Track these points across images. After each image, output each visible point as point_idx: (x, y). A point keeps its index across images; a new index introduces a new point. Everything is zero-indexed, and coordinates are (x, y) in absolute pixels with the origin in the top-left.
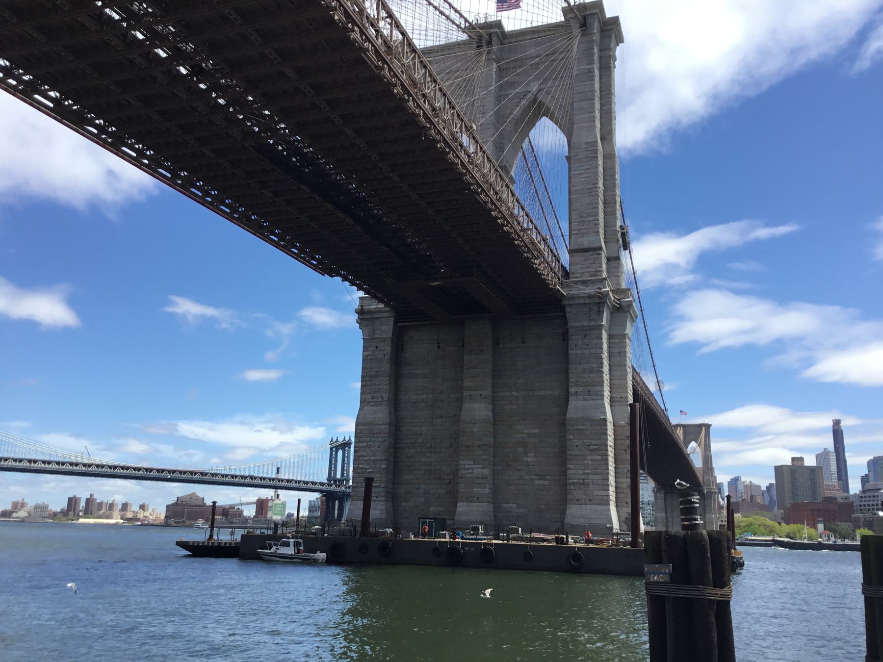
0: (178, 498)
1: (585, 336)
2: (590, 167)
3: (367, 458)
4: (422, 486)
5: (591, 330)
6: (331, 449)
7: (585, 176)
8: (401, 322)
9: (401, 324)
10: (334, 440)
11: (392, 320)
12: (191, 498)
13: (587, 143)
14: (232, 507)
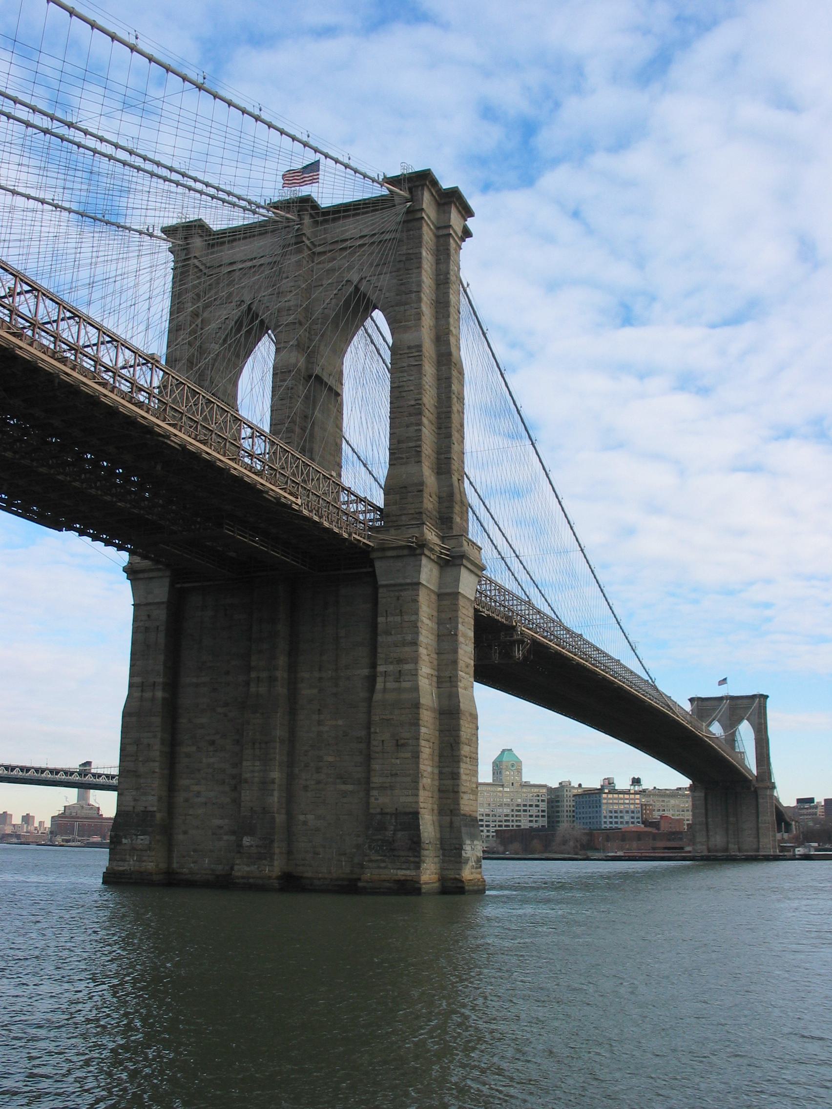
0: (65, 807)
1: (398, 599)
5: (405, 590)
8: (178, 583)
9: (178, 586)
11: (166, 582)
13: (409, 348)
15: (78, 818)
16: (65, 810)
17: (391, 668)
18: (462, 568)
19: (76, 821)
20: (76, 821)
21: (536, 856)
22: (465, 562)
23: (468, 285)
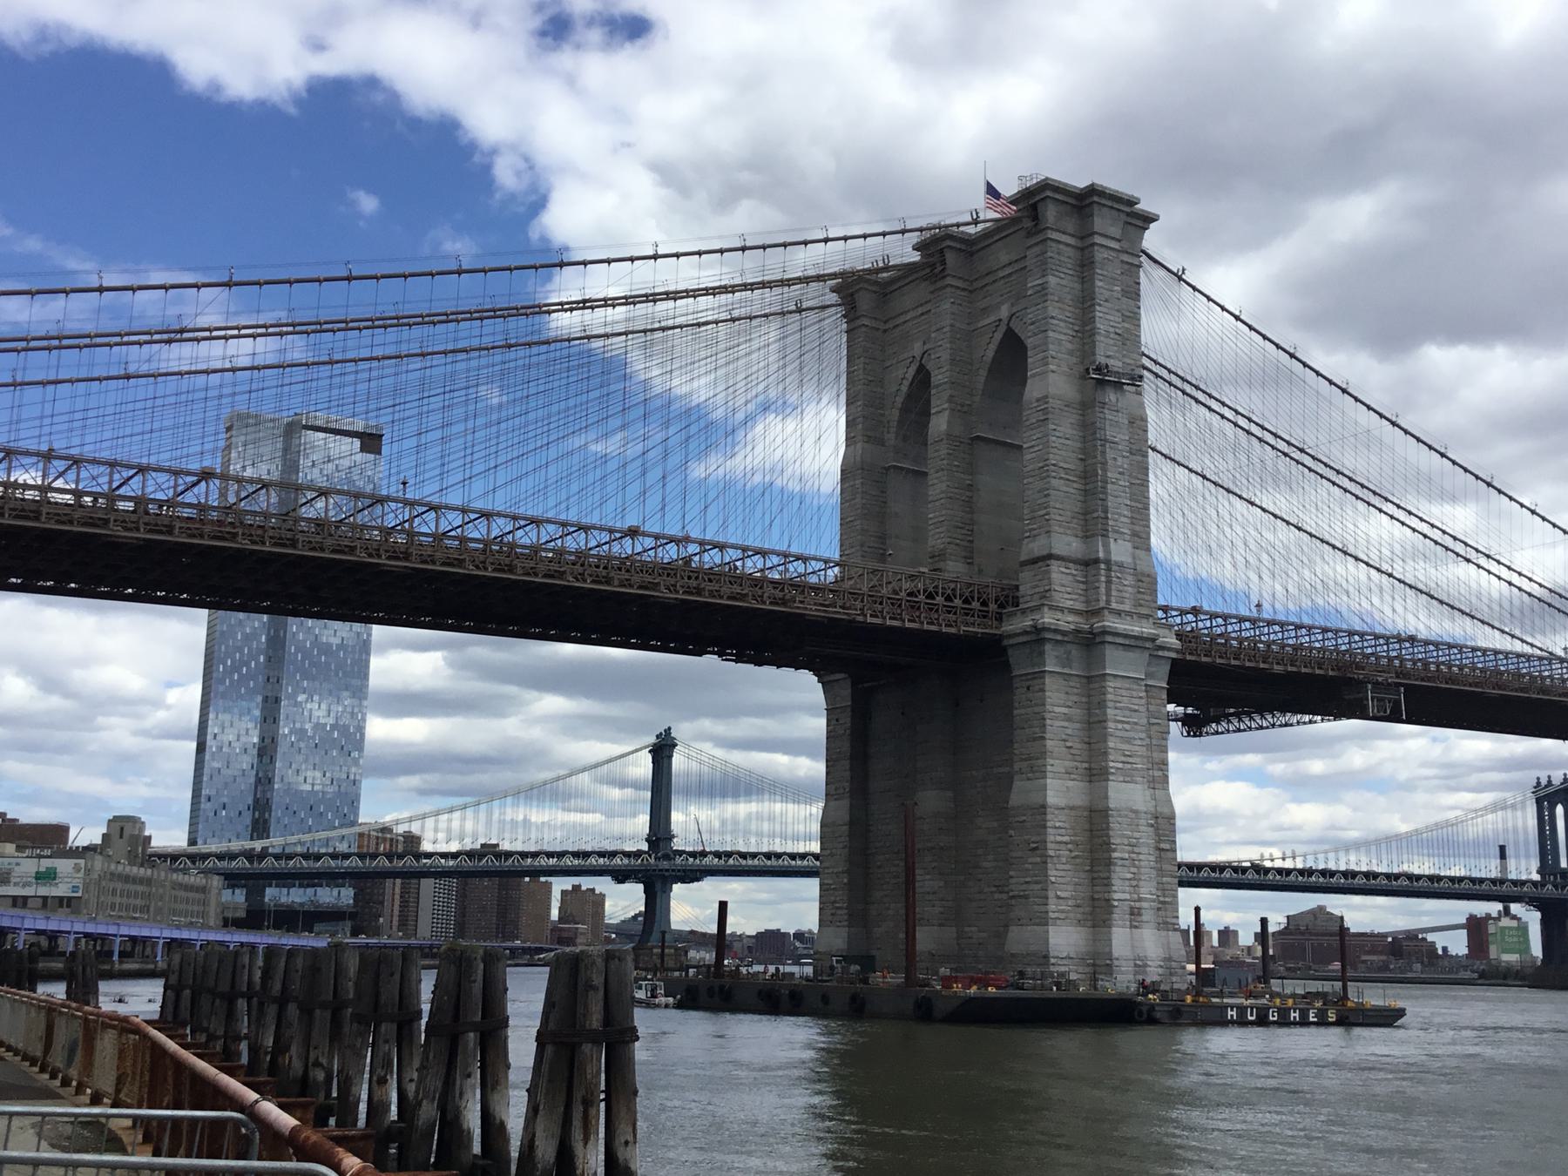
0: (1288, 917)
1: (1028, 688)
2: (1039, 436)
3: (830, 870)
4: (893, 905)
5: (1035, 678)
6: (1539, 802)
7: (1036, 449)
9: (860, 686)
10: (1544, 782)
11: (849, 682)
12: (1316, 918)
13: (1038, 400)
14: (1412, 936)
15: (1311, 934)
16: (1288, 923)
17: (1026, 763)
18: (1107, 645)
19: (1309, 940)
20: (1309, 940)
21: (1493, 981)
22: (1109, 638)
23: (1184, 270)
